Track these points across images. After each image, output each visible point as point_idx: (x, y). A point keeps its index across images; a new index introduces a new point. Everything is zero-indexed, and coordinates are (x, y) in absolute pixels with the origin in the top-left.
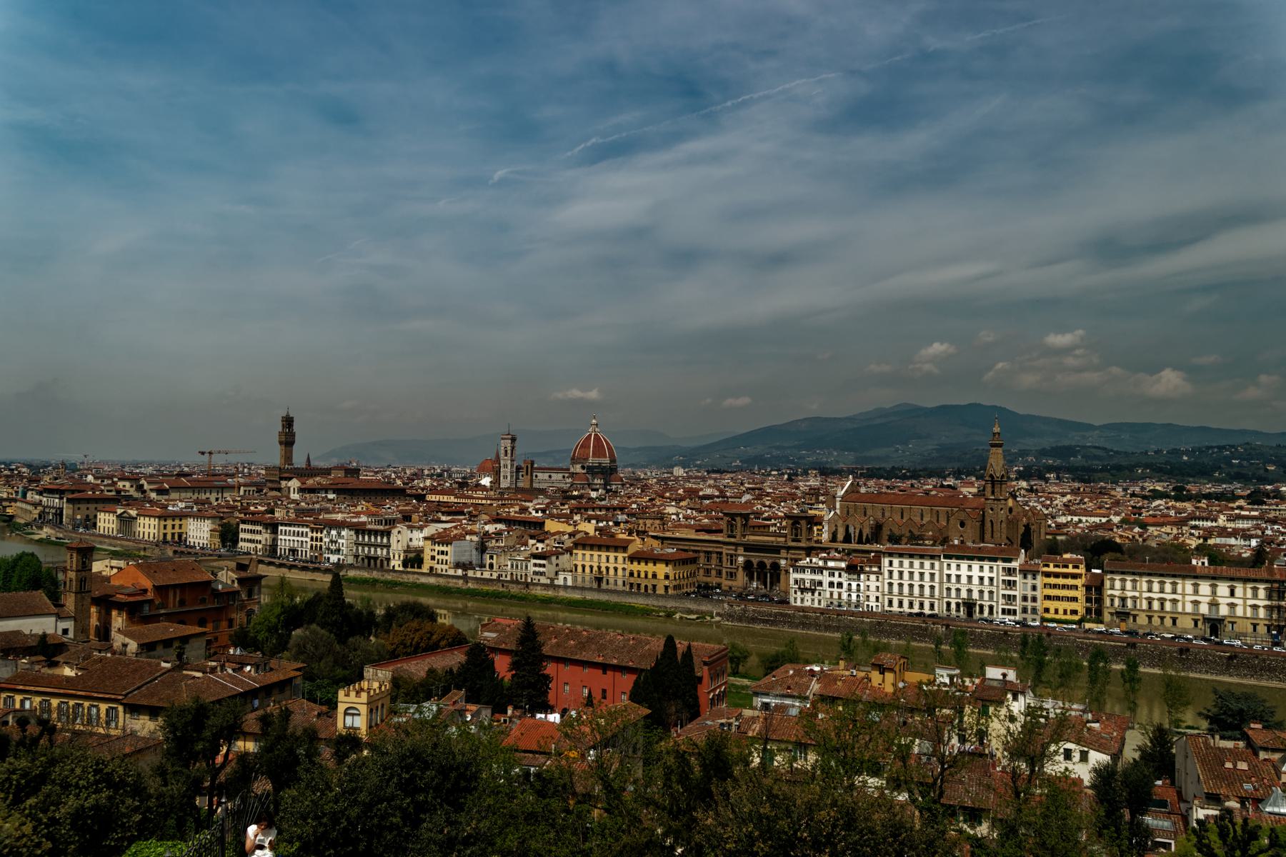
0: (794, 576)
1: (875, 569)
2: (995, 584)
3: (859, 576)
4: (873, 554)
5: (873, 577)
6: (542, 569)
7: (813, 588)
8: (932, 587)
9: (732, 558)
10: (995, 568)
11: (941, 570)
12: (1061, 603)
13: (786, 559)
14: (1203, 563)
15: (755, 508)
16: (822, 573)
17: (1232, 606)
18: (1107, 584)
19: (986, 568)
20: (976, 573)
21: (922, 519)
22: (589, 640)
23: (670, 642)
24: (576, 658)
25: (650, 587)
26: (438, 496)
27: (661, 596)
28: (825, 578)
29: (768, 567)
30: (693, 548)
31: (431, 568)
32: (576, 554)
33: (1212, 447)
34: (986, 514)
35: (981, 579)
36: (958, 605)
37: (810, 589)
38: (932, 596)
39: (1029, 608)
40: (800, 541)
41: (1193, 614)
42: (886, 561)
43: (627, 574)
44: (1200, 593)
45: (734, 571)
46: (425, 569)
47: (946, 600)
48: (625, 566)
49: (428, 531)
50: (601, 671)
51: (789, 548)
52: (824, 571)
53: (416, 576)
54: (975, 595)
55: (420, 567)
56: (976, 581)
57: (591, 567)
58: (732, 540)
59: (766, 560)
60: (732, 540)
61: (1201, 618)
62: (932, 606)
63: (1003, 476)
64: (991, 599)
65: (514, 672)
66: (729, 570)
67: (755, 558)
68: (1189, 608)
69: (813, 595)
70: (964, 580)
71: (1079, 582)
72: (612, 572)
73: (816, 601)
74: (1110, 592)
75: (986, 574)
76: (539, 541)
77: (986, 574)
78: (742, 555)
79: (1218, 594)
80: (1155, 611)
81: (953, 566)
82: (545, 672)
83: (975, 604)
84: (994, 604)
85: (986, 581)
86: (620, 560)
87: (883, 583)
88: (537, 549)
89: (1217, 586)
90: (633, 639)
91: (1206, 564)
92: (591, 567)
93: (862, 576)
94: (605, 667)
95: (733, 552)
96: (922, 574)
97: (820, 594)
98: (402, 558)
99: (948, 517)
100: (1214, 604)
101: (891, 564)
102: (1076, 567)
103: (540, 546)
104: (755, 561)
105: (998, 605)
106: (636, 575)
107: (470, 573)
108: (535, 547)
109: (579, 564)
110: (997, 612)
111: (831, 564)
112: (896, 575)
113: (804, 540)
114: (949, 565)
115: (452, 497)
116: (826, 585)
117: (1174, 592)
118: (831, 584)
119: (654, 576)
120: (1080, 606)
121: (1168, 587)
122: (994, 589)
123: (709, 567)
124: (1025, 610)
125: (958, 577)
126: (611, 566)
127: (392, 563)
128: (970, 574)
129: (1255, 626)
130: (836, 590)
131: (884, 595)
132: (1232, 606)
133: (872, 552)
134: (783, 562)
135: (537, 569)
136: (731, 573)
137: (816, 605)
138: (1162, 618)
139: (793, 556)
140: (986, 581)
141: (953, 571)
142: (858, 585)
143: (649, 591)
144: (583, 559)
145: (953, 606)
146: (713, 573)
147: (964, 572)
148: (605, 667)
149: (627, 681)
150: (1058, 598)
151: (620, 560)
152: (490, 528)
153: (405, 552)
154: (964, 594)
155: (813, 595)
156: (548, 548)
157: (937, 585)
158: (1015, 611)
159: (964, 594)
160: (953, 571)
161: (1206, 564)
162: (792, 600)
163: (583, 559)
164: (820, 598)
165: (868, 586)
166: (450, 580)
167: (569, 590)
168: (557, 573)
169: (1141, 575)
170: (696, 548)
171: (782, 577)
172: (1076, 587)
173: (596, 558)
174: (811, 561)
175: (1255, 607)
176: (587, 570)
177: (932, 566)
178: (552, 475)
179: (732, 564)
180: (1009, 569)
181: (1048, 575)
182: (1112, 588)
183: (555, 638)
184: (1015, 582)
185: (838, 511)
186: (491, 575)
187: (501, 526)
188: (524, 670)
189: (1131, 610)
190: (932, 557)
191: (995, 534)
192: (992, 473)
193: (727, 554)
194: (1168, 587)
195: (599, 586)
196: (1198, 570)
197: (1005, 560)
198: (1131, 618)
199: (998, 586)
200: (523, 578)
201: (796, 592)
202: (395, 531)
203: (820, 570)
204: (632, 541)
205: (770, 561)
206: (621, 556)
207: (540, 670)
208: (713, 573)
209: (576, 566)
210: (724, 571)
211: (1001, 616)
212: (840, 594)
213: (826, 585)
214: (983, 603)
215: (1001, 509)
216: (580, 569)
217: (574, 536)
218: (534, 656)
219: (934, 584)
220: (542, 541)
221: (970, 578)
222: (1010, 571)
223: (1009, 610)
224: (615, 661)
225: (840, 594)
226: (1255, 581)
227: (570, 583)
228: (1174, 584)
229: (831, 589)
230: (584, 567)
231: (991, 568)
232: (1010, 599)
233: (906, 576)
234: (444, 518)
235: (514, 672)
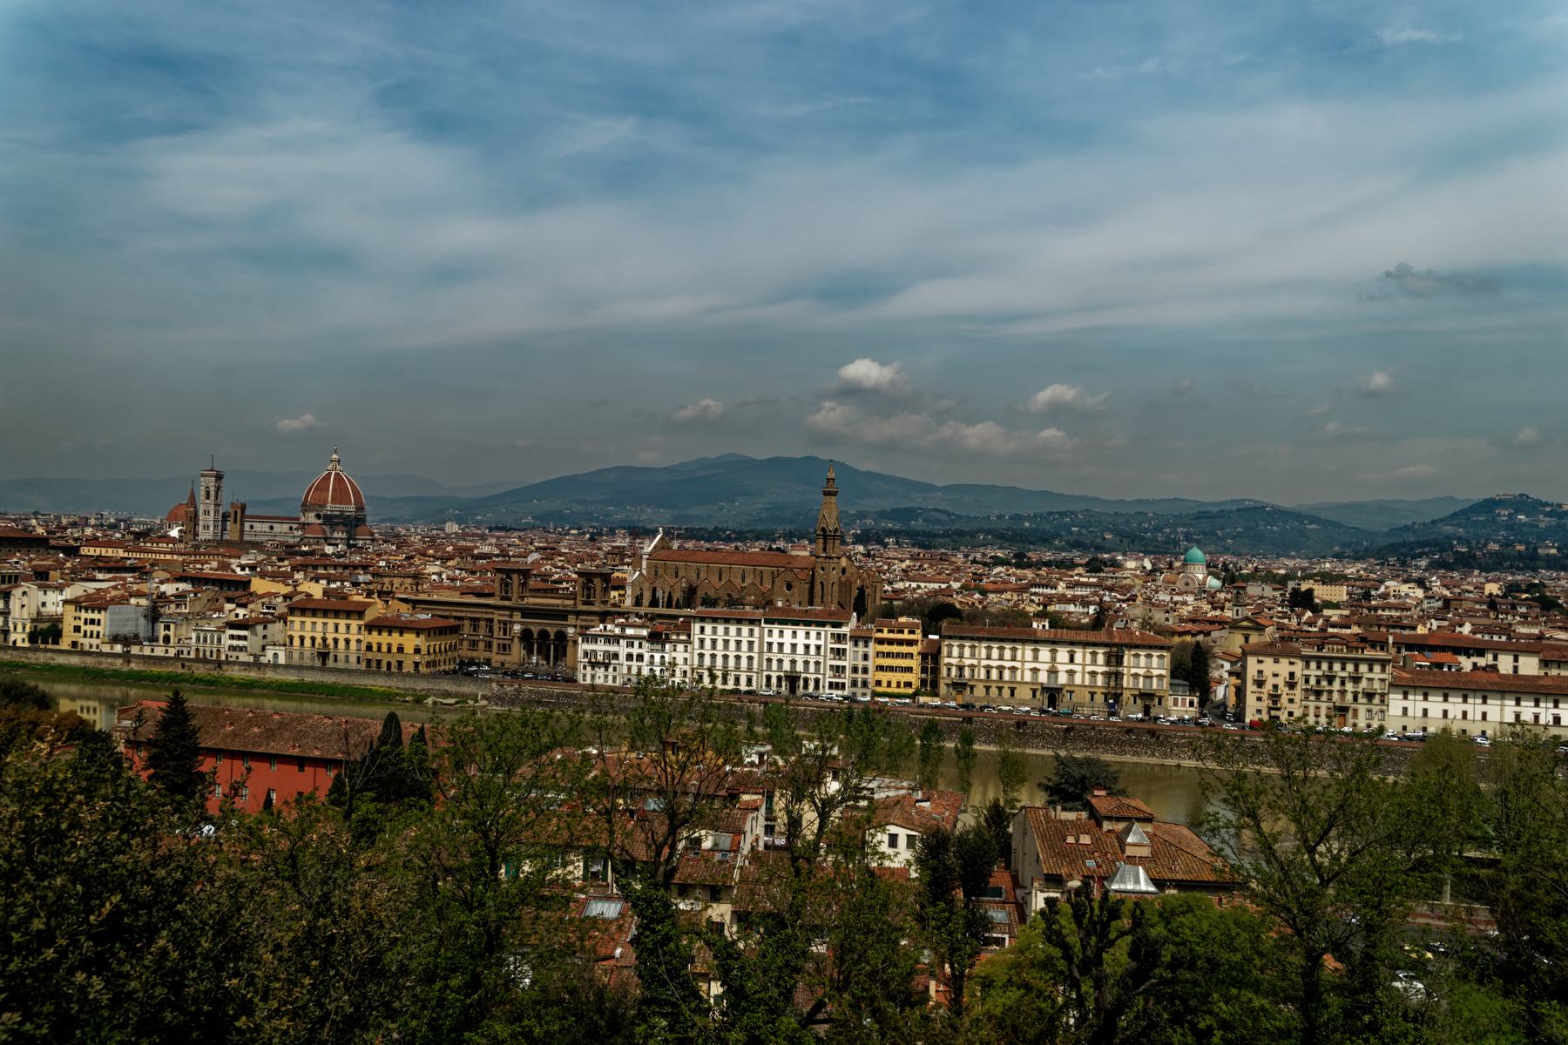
0: (583, 647)
1: (683, 637)
3: (664, 646)
5: (680, 647)
6: (241, 643)
10: (823, 634)
11: (761, 638)
13: (575, 626)
17: (1071, 673)
18: (945, 651)
19: (813, 634)
20: (801, 640)
22: (282, 726)
23: (392, 722)
24: (261, 750)
25: (394, 664)
26: (98, 549)
27: (409, 674)
28: (622, 649)
30: (454, 614)
31: (74, 644)
32: (292, 622)
35: (807, 647)
36: (779, 678)
37: (603, 663)
38: (750, 669)
41: (1033, 683)
42: (696, 627)
43: (363, 647)
45: (507, 642)
46: (65, 644)
47: (765, 673)
48: (361, 637)
49: (69, 593)
50: (296, 768)
51: (578, 613)
53: (49, 655)
55: (56, 642)
56: (801, 650)
57: (313, 639)
58: (507, 603)
59: (549, 629)
60: (507, 603)
62: (749, 681)
63: (836, 530)
64: (817, 671)
65: (152, 771)
67: (536, 626)
68: (1028, 677)
70: (787, 649)
71: (914, 650)
72: (342, 645)
73: (610, 678)
74: (947, 660)
75: (813, 641)
76: (239, 605)
77: (813, 641)
81: (776, 632)
82: (201, 769)
84: (820, 677)
85: (813, 650)
86: (354, 629)
87: (692, 654)
88: (237, 615)
90: (346, 722)
92: (313, 639)
93: (668, 646)
94: (301, 762)
95: (507, 619)
96: (738, 643)
97: (615, 669)
98: (28, 630)
100: (1053, 672)
101: (702, 630)
102: (912, 632)
103: (241, 612)
104: (535, 630)
106: (375, 648)
107: (135, 650)
108: (233, 613)
109: (296, 635)
111: (630, 631)
112: (708, 644)
113: (597, 604)
114: (770, 631)
115: (120, 551)
116: (622, 657)
118: (630, 657)
119: (401, 649)
120: (914, 678)
122: (822, 660)
124: (854, 683)
125: (781, 645)
126: (341, 637)
127: (13, 637)
128: (794, 641)
129: (1092, 694)
130: (635, 664)
131: (693, 670)
132: (1071, 673)
134: (571, 631)
135: (235, 643)
136: (504, 646)
137: (610, 683)
138: (1000, 689)
140: (813, 650)
142: (663, 657)
143: (394, 669)
144: (302, 628)
145: (774, 681)
146: (481, 645)
147: (787, 639)
148: (301, 762)
149: (327, 778)
150: (891, 669)
151: (354, 629)
152: (169, 589)
153: (33, 621)
154: (787, 666)
156: (253, 615)
157: (756, 656)
158: (843, 685)
159: (787, 666)
160: (775, 639)
163: (302, 628)
166: (103, 660)
167: (280, 670)
168: (264, 648)
169: (980, 639)
170: (459, 614)
171: (570, 649)
172: (911, 656)
173: (319, 627)
175: (1093, 674)
176: (308, 643)
177: (751, 633)
178: (275, 525)
179: (505, 634)
180: (839, 635)
181: (881, 642)
182: (949, 656)
183: (231, 724)
184: (844, 650)
185: (644, 572)
186: (167, 651)
187: (183, 586)
188: (168, 767)
190: (752, 622)
193: (499, 622)
194: (1008, 654)
195: (324, 663)
196: (1039, 634)
197: (835, 625)
199: (825, 656)
200: (215, 655)
201: (585, 668)
202: (17, 592)
203: (615, 639)
204: (370, 604)
205: (555, 629)
206: (354, 624)
207: (194, 767)
208: (481, 645)
209: (291, 638)
210: (495, 643)
211: (827, 691)
212: (640, 669)
213: (622, 657)
216: (297, 642)
217: (291, 598)
218: (183, 746)
220: (244, 606)
221: (794, 646)
222: (839, 638)
223: (837, 684)
224: (317, 753)
225: (640, 669)
226: (1095, 645)
227: (282, 660)
228: (1014, 650)
230: (302, 639)
231: (819, 634)
232: (838, 670)
233: (720, 645)
234: (100, 576)
235: (152, 771)
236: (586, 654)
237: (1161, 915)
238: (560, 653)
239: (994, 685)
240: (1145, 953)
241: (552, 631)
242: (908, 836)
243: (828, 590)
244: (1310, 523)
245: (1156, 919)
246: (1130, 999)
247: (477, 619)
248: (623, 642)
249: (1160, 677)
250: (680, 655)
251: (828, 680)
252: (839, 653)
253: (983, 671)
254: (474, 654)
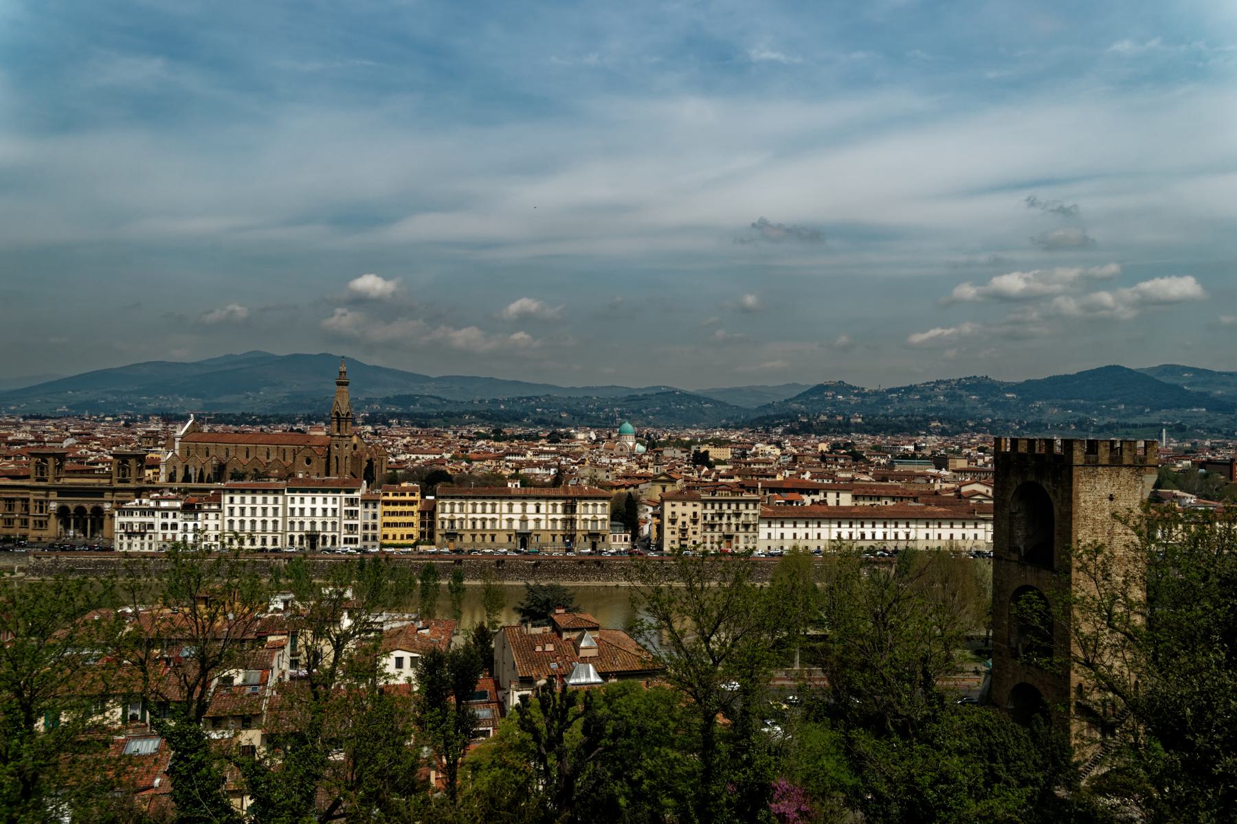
0: (119, 519)
2: (338, 515)
3: (196, 515)
4: (212, 492)
5: (212, 516)
7: (143, 531)
8: (275, 522)
9: (42, 505)
10: (338, 499)
11: (285, 505)
12: (398, 529)
13: (112, 502)
14: (516, 486)
15: (79, 453)
16: (153, 515)
17: (538, 521)
18: (439, 508)
19: (330, 500)
20: (319, 505)
21: (268, 458)
28: (158, 520)
29: (89, 512)
33: (522, 398)
34: (332, 451)
35: (325, 510)
36: (301, 538)
37: (139, 533)
38: (275, 530)
39: (370, 535)
40: (129, 482)
41: (508, 530)
44: (514, 512)
47: (289, 534)
51: (114, 491)
52: (156, 513)
54: (319, 527)
56: (319, 513)
58: (42, 484)
59: (85, 505)
60: (42, 484)
61: (513, 533)
62: (275, 541)
63: (348, 414)
64: (334, 529)
66: (37, 519)
67: (72, 503)
68: (505, 525)
69: (142, 539)
70: (308, 512)
71: (414, 508)
73: (146, 546)
74: (441, 516)
77: (330, 505)
78: (55, 501)
79: (528, 512)
80: (479, 530)
81: (297, 499)
83: (318, 536)
84: (337, 534)
85: (330, 513)
87: (223, 520)
89: (526, 504)
91: (519, 486)
93: (200, 515)
96: (265, 510)
97: (150, 538)
99: (294, 454)
100: (524, 521)
101: (232, 500)
102: (412, 494)
104: (72, 507)
105: (340, 535)
110: (340, 542)
111: (164, 504)
112: (237, 512)
113: (133, 481)
117: (493, 512)
120: (414, 531)
121: (489, 508)
122: (337, 521)
123: (13, 517)
124: (365, 538)
125: (302, 510)
128: (313, 506)
129: (554, 536)
132: (538, 521)
133: (212, 489)
134: (107, 506)
136: (41, 523)
137: (146, 549)
138: (483, 536)
139: (120, 499)
140: (330, 513)
141: (297, 505)
142: (196, 525)
145: (297, 539)
146: (17, 523)
147: (308, 504)
150: (396, 525)
154: (307, 527)
155: (142, 539)
157: (280, 520)
158: (356, 540)
159: (307, 527)
160: (297, 505)
161: (519, 486)
162: (117, 547)
164: (150, 541)
165: (207, 525)
169: (467, 498)
171: (106, 522)
172: (412, 513)
174: (141, 502)
175: (554, 520)
177: (276, 501)
179: (41, 511)
180: (352, 499)
181: (387, 503)
182: (443, 512)
184: (357, 511)
185: (177, 452)
189: (458, 530)
190: (276, 492)
192: (338, 410)
193: (35, 501)
194: (489, 508)
196: (512, 492)
197: (348, 492)
198: (458, 538)
199: (340, 517)
201: (121, 538)
203: (152, 512)
205: (92, 505)
208: (17, 523)
211: (343, 545)
212: (174, 536)
213: (157, 527)
214: (326, 534)
215: (346, 445)
219: (277, 519)
221: (313, 510)
222: (352, 502)
223: (351, 539)
225: (174, 536)
228: (494, 505)
229: (164, 532)
231: (335, 499)
232: (352, 528)
233: (248, 512)
236: (122, 526)
237: (605, 699)
238: (97, 525)
239: (478, 533)
240: (593, 729)
241: (88, 507)
242: (411, 658)
243: (342, 462)
244: (706, 403)
245: (602, 702)
246: (583, 765)
247: (14, 500)
248: (158, 514)
249: (603, 520)
250: (212, 521)
251: (343, 537)
252: (353, 514)
253: (470, 523)
254: (10, 531)
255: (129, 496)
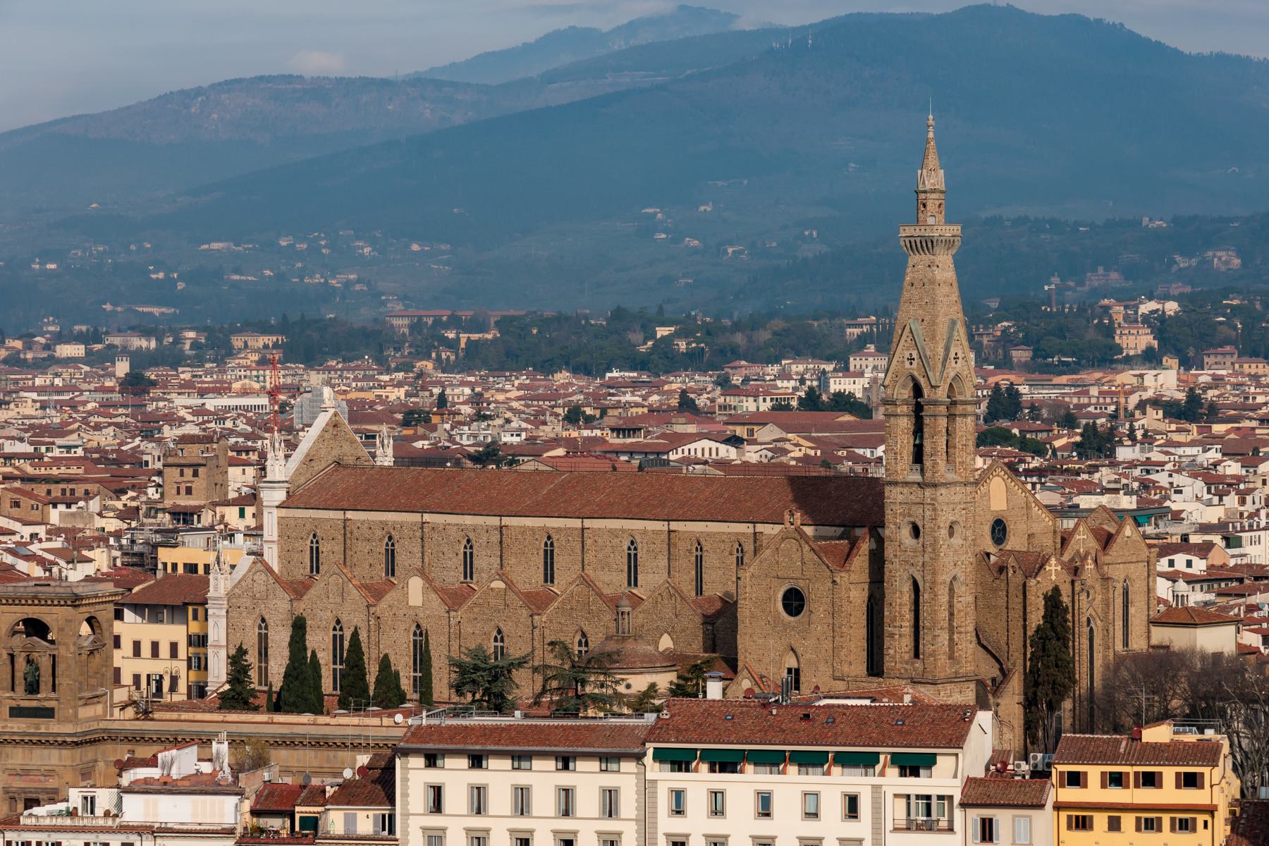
21: (633, 580)
34: (889, 552)
40: (48, 713)
99: (740, 562)
114: (678, 795)
174: (90, 803)
191: (926, 638)
192: (915, 368)
197: (911, 767)
243: (937, 608)
255: (50, 773)
